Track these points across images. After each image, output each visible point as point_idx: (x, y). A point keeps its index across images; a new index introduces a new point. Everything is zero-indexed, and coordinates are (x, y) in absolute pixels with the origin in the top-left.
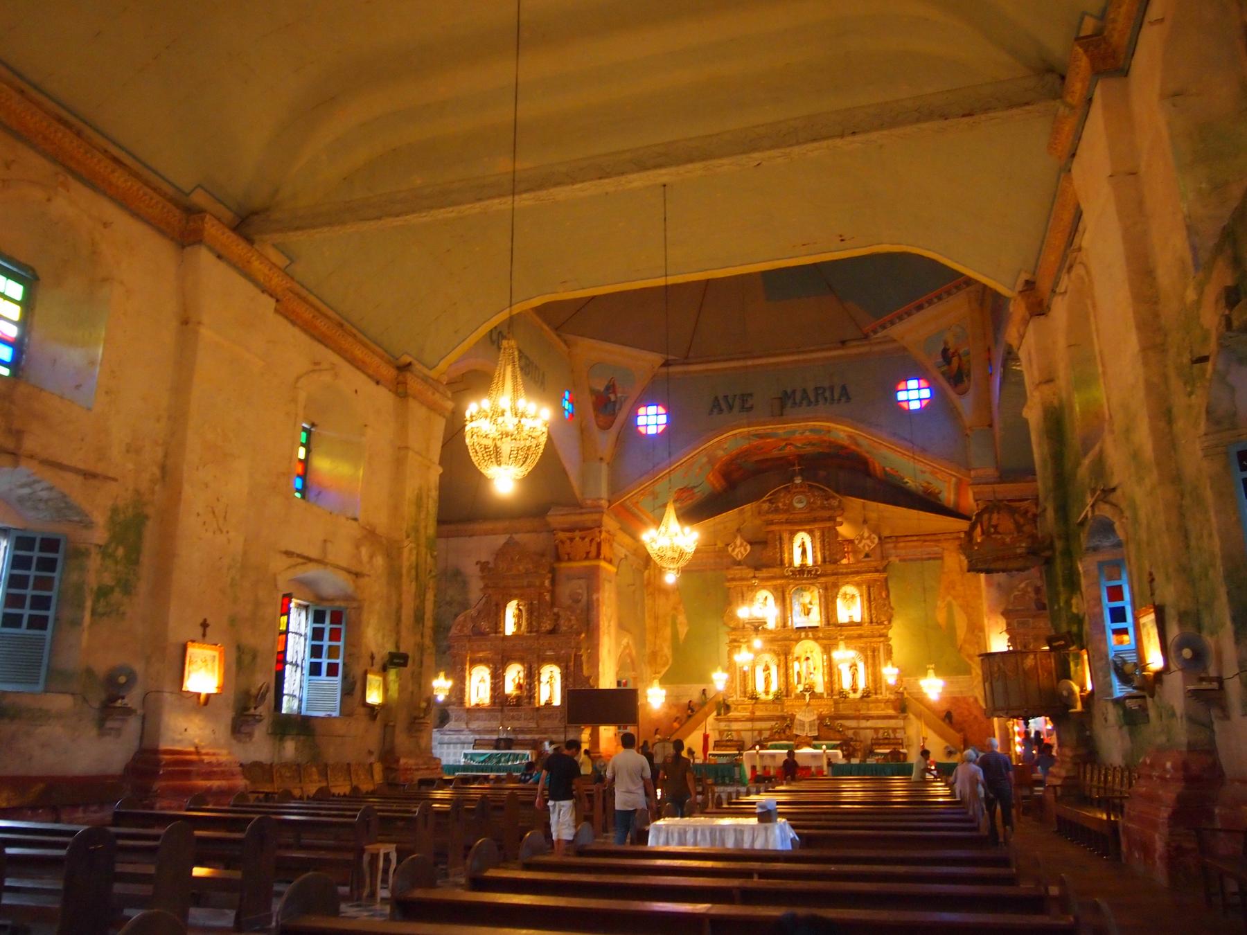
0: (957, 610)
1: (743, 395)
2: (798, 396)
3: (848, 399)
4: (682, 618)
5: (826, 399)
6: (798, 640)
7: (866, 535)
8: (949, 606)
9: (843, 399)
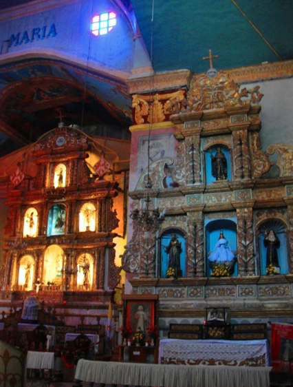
3: (56, 34)
6: (48, 244)
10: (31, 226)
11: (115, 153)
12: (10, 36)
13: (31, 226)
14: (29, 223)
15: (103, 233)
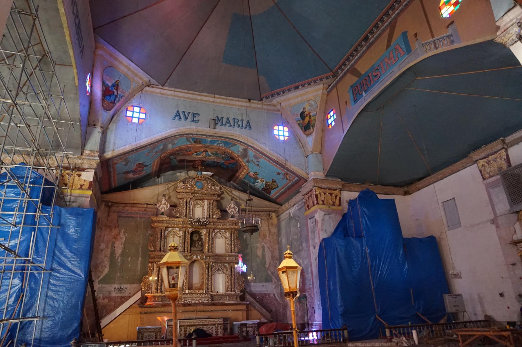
0: (266, 249)
1: (194, 114)
2: (224, 120)
5: (239, 125)
7: (232, 206)
8: (263, 247)
9: (248, 127)
12: (216, 116)
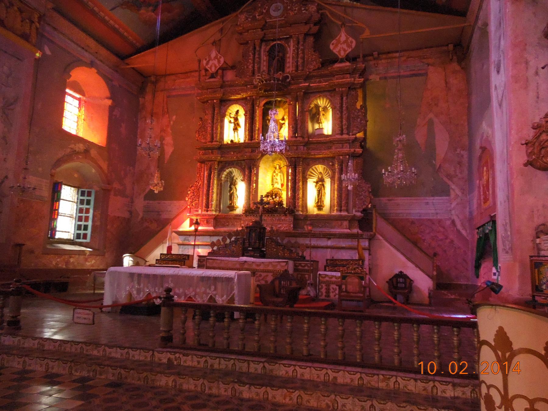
4: (169, 140)
8: (430, 123)
10: (235, 129)
11: (364, 26)
13: (235, 129)
14: (233, 125)
15: (345, 136)
